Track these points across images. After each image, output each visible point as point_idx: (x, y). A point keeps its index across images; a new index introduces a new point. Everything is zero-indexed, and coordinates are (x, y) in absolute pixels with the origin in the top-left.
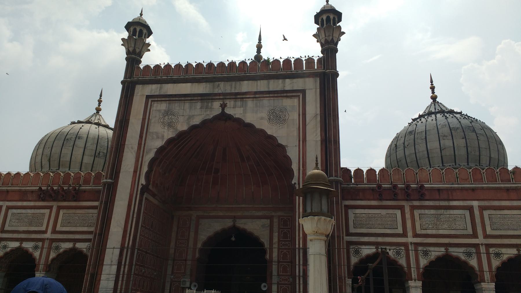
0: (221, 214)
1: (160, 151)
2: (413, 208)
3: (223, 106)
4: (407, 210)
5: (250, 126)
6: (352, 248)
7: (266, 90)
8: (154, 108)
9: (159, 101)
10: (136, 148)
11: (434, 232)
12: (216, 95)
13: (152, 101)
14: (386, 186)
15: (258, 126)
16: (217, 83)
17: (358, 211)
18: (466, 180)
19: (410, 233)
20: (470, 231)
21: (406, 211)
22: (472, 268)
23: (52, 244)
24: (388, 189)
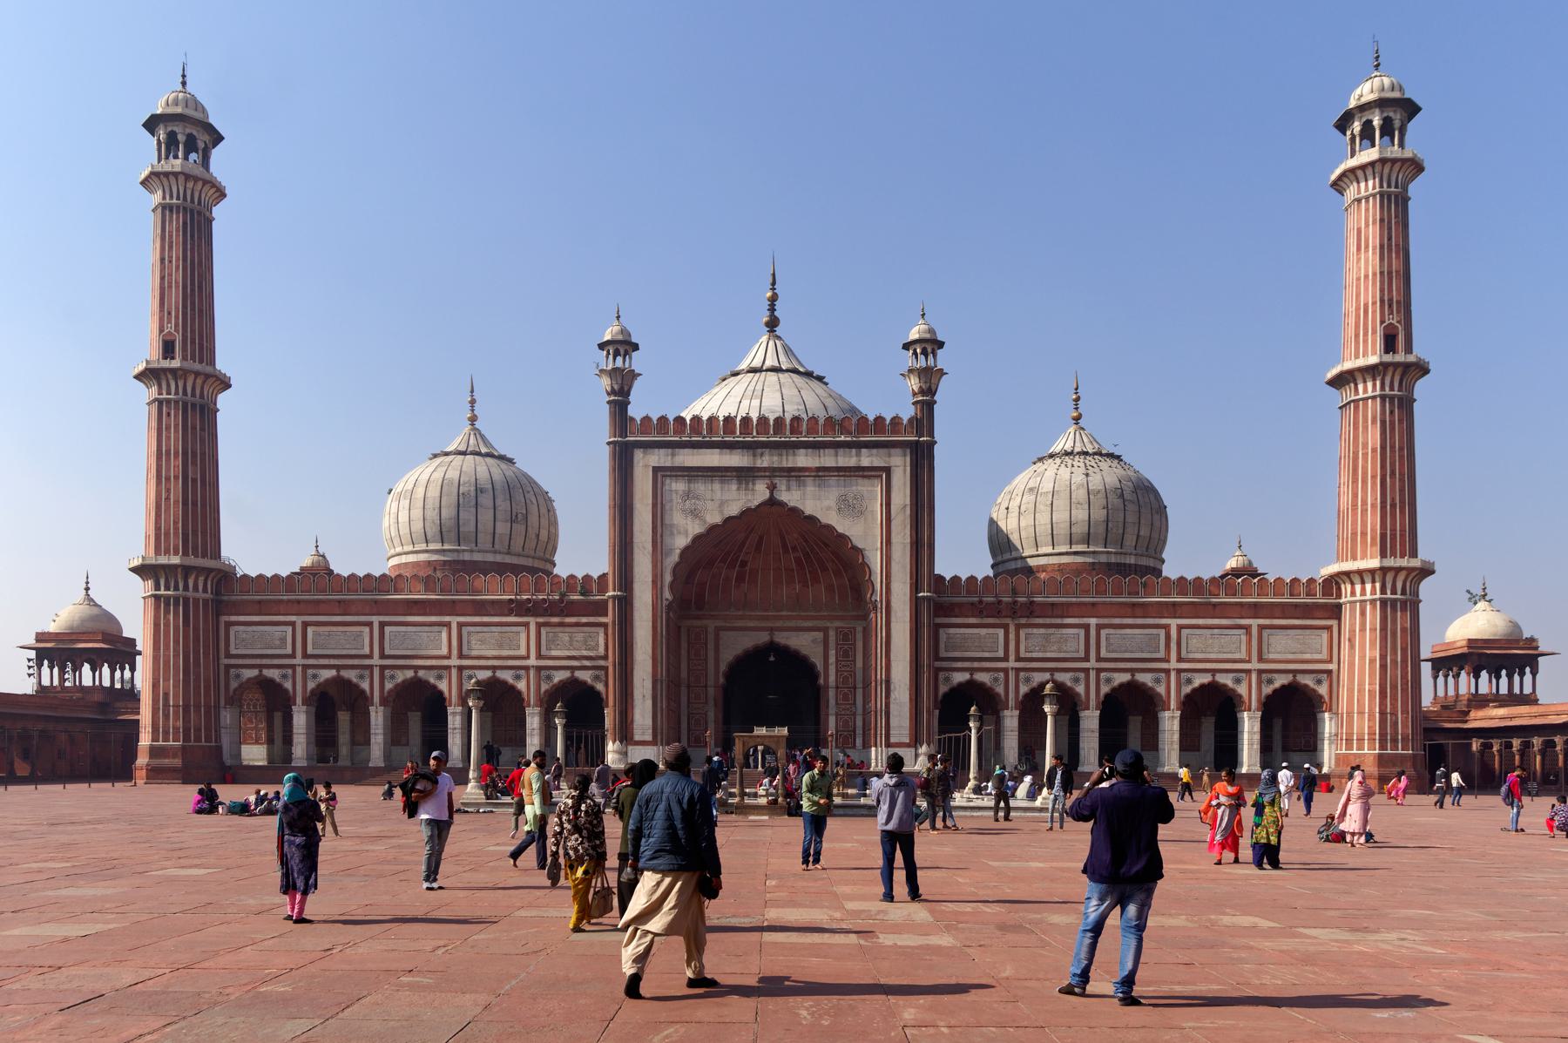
0: (751, 624)
1: (685, 551)
2: (1018, 627)
3: (772, 488)
4: (1012, 629)
5: (812, 519)
6: (942, 675)
7: (834, 465)
8: (667, 487)
9: (676, 476)
10: (651, 548)
11: (1040, 655)
12: (760, 469)
13: (663, 476)
14: (989, 599)
15: (824, 520)
16: (759, 451)
17: (952, 631)
18: (1087, 592)
19: (1012, 657)
20: (1082, 655)
21: (1010, 631)
22: (1078, 694)
23: (540, 673)
24: (993, 603)
